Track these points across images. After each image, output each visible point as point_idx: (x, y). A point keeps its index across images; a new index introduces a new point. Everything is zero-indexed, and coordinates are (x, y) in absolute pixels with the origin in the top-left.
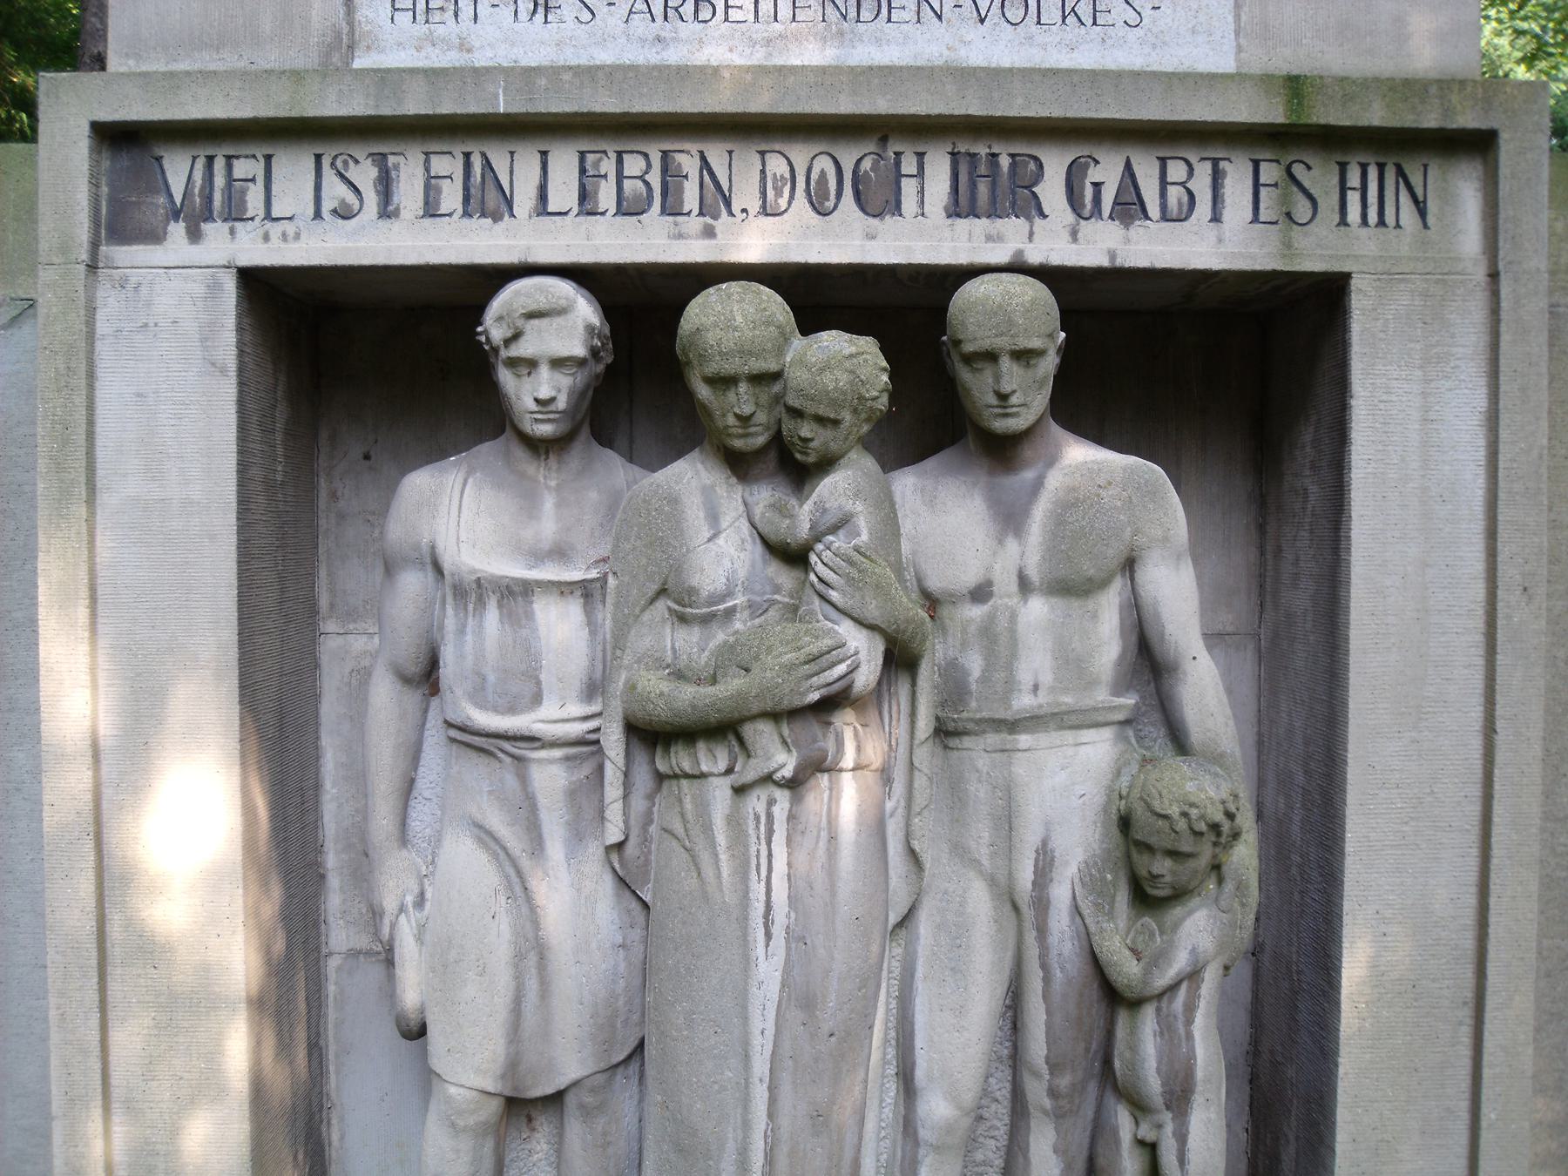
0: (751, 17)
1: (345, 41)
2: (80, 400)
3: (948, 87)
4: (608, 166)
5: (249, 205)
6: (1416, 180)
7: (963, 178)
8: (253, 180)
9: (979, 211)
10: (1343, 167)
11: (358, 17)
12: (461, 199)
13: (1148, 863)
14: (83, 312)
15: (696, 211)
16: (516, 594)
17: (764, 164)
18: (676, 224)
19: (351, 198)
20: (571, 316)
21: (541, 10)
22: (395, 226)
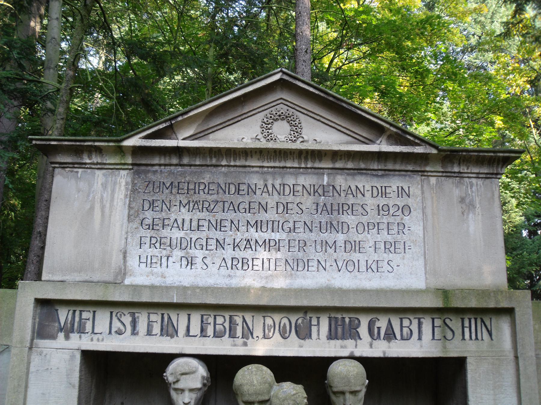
0: (261, 269)
1: (123, 272)
2: (21, 396)
3: (328, 296)
4: (211, 320)
5: (87, 328)
6: (488, 323)
7: (333, 326)
8: (88, 319)
9: (338, 337)
10: (463, 320)
11: (128, 264)
12: (160, 329)
14: (26, 365)
15: (241, 337)
17: (264, 321)
18: (234, 341)
19: (122, 328)
20: (197, 374)
21: (190, 264)
22: (137, 338)
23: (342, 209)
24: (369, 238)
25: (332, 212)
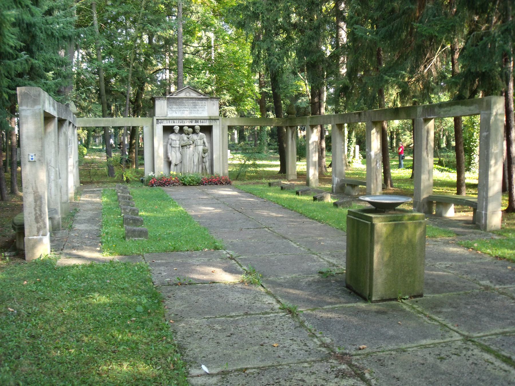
1: (167, 115)
13: (204, 151)
16: (176, 140)
23: (196, 105)
24: (200, 109)
25: (195, 106)
